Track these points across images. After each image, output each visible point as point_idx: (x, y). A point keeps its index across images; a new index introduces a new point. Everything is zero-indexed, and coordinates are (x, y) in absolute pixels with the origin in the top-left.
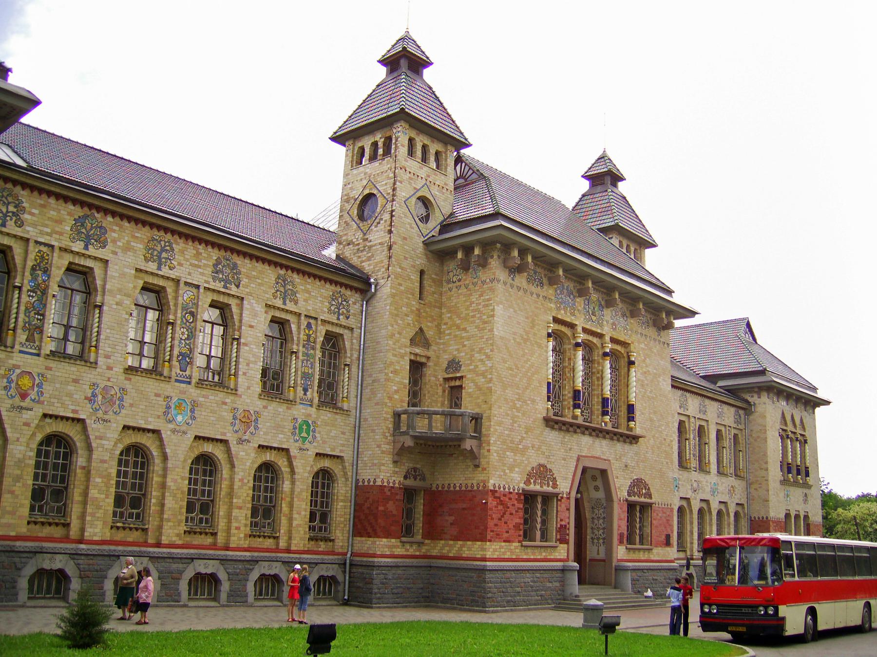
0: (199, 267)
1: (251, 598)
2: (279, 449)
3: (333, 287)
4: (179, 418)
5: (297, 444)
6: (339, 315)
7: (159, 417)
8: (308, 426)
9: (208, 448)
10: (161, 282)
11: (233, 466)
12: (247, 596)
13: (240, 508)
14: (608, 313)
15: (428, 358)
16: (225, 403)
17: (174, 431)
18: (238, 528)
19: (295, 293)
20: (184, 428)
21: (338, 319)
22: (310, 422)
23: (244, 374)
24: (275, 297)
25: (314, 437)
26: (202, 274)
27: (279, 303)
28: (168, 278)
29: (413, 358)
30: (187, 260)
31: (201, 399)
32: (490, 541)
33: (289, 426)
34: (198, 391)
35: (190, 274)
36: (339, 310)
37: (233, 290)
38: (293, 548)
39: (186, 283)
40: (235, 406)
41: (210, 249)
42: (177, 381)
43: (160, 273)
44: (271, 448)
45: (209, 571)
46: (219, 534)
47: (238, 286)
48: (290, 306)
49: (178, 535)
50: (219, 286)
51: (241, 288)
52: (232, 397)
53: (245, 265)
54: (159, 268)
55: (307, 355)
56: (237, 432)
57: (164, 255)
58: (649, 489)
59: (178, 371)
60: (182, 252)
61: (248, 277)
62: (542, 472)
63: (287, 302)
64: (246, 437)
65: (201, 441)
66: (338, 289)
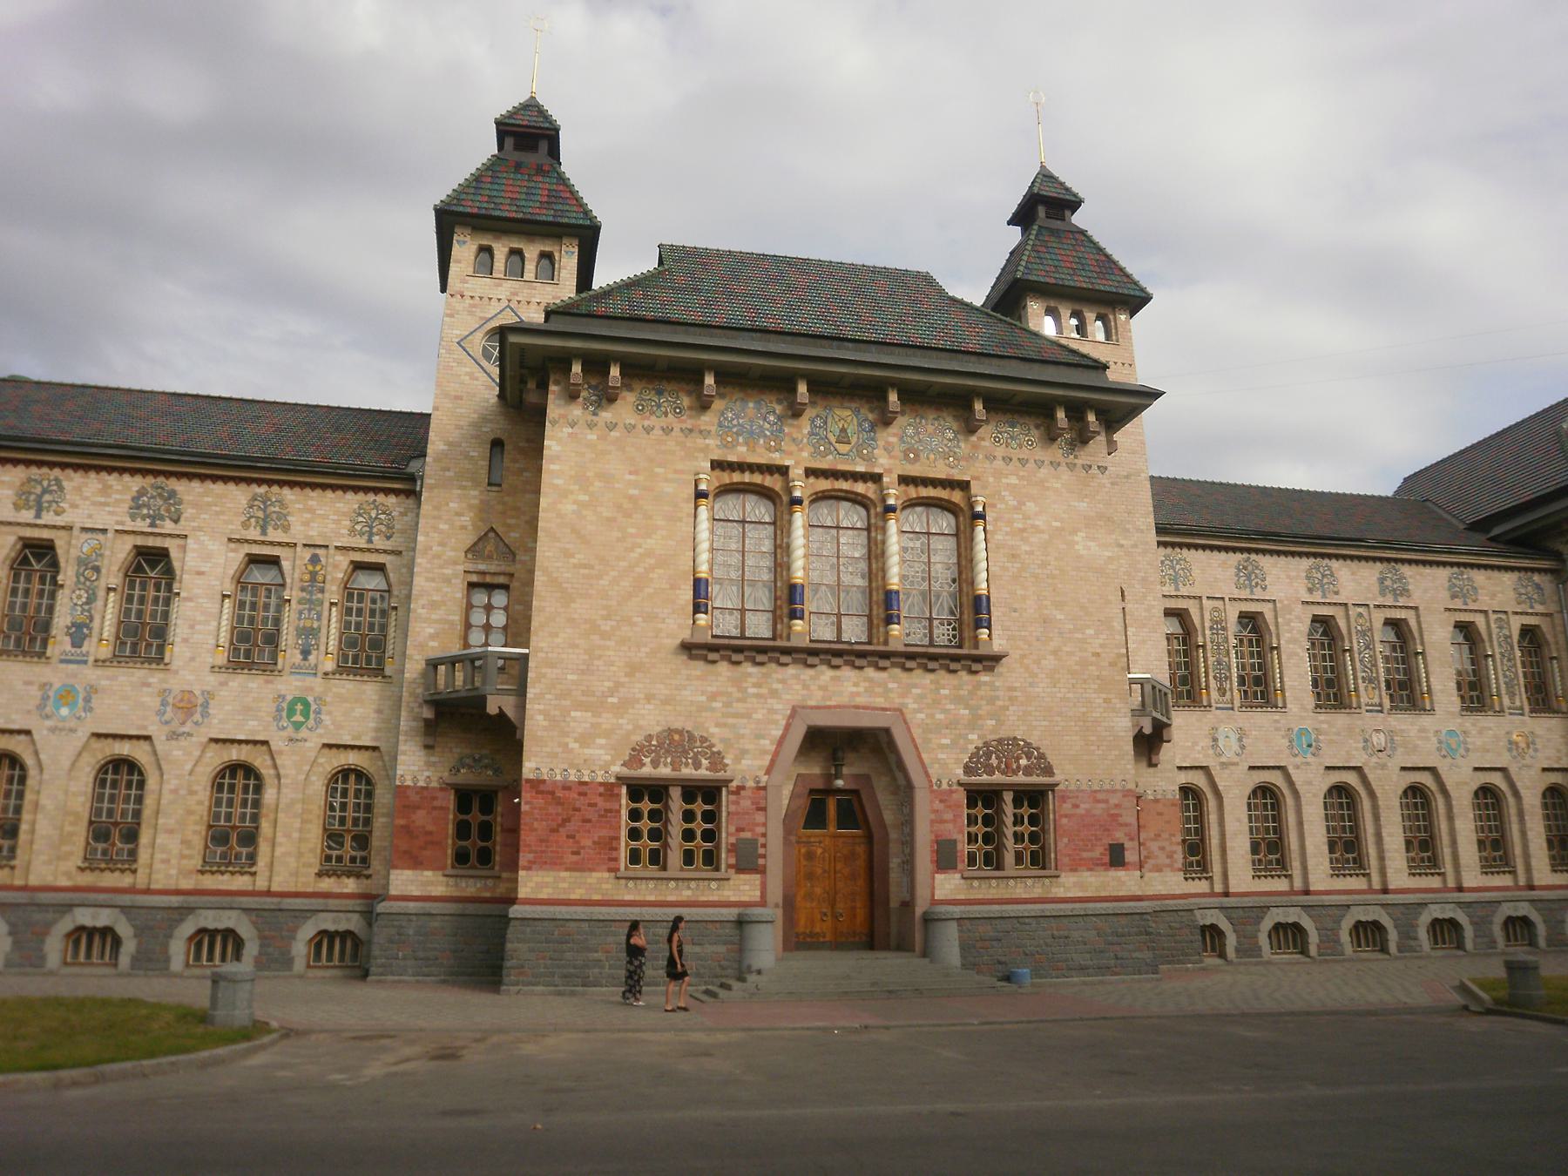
0: (107, 504)
1: (299, 965)
2: (247, 742)
3: (361, 496)
4: (64, 711)
5: (284, 734)
6: (371, 534)
7: (29, 712)
8: (306, 704)
9: (124, 749)
10: (45, 534)
11: (41, 770)
12: (168, 960)
13: (171, 832)
14: (889, 436)
15: (512, 575)
16: (148, 685)
17: (53, 730)
18: (166, 861)
19: (282, 516)
20: (73, 724)
21: (370, 541)
22: (310, 699)
23: (185, 640)
24: (245, 525)
25: (319, 722)
26: (110, 513)
27: (254, 534)
28: (54, 527)
29: (474, 578)
30: (86, 498)
31: (103, 682)
32: (528, 869)
33: (268, 707)
34: (99, 672)
35: (90, 516)
36: (371, 527)
37: (168, 526)
38: (275, 888)
39: (84, 529)
40: (165, 686)
41: (127, 477)
42: (62, 661)
43: (39, 522)
44: (233, 741)
45: (100, 923)
46: (140, 871)
47: (176, 521)
48: (274, 535)
49: (68, 874)
50: (142, 525)
51: (182, 522)
52: (161, 675)
53: (189, 491)
54: (38, 516)
55: (310, 601)
56: (167, 723)
57: (47, 497)
58: (1042, 756)
59: (68, 648)
60: (78, 489)
61: (196, 505)
62: (676, 742)
63: (270, 530)
64: (185, 729)
65: (110, 741)
66: (371, 497)
